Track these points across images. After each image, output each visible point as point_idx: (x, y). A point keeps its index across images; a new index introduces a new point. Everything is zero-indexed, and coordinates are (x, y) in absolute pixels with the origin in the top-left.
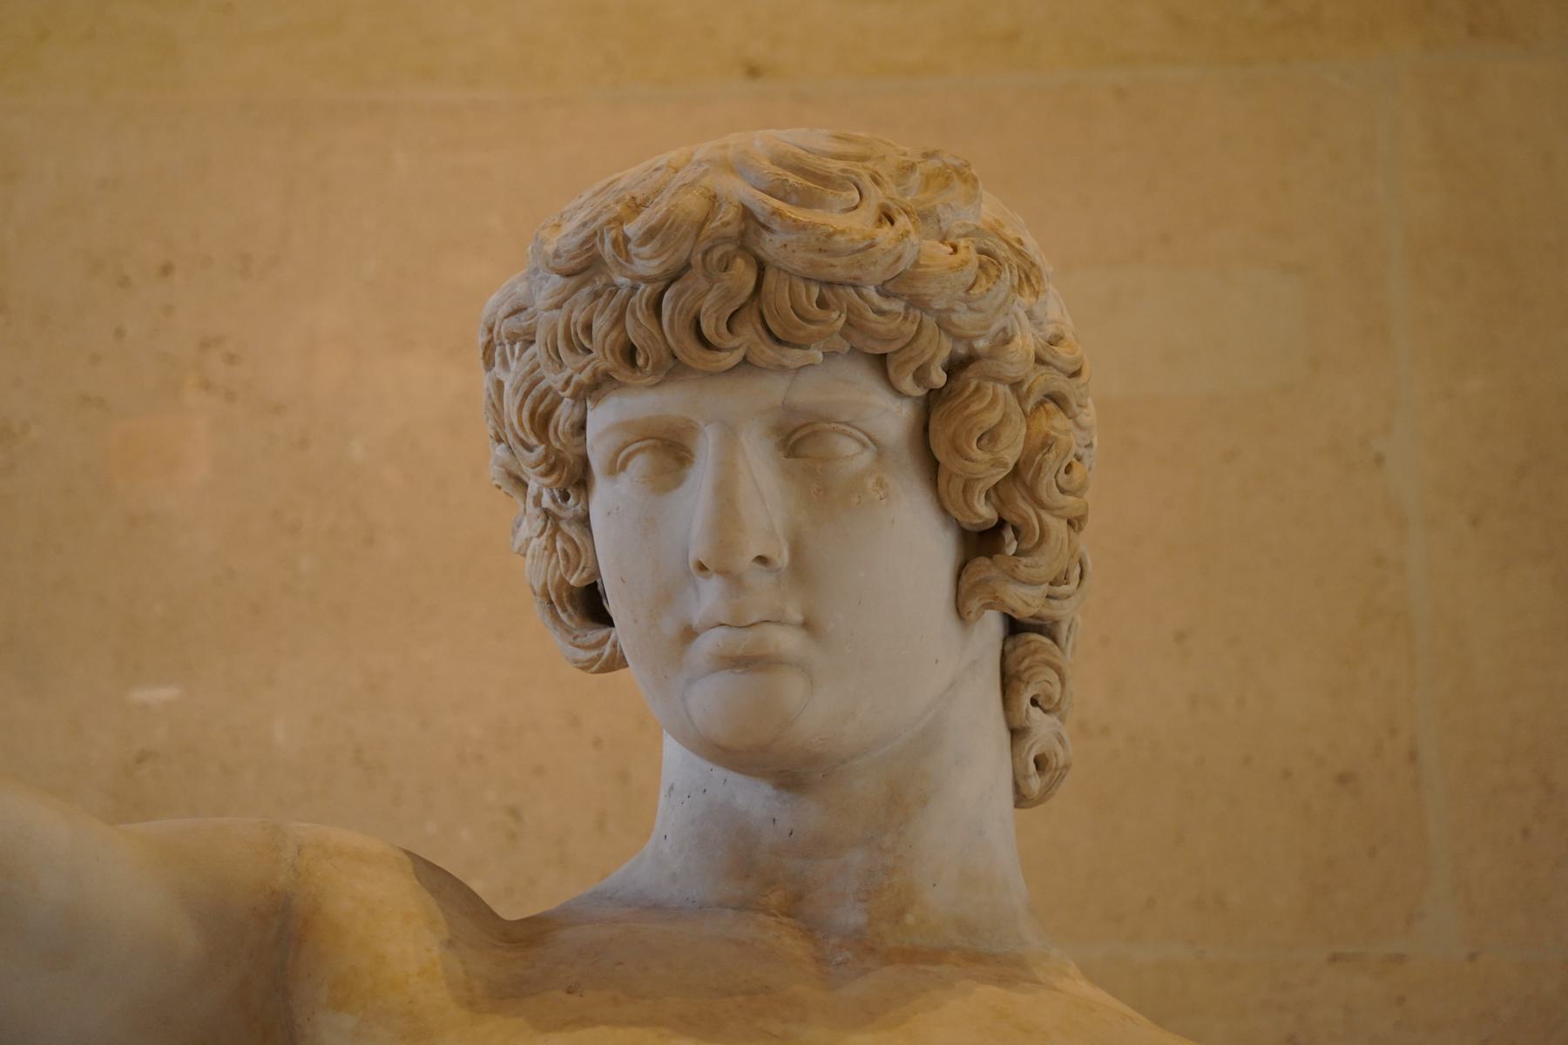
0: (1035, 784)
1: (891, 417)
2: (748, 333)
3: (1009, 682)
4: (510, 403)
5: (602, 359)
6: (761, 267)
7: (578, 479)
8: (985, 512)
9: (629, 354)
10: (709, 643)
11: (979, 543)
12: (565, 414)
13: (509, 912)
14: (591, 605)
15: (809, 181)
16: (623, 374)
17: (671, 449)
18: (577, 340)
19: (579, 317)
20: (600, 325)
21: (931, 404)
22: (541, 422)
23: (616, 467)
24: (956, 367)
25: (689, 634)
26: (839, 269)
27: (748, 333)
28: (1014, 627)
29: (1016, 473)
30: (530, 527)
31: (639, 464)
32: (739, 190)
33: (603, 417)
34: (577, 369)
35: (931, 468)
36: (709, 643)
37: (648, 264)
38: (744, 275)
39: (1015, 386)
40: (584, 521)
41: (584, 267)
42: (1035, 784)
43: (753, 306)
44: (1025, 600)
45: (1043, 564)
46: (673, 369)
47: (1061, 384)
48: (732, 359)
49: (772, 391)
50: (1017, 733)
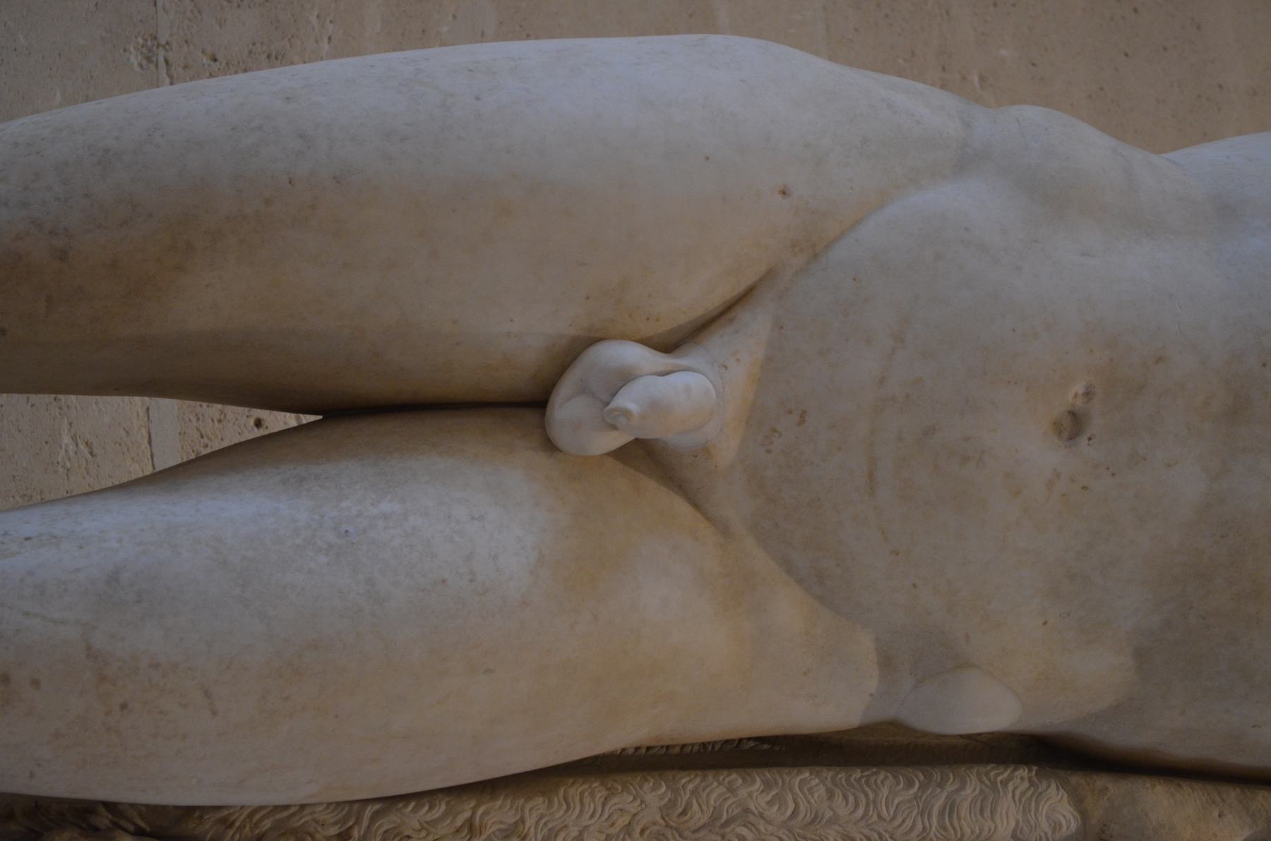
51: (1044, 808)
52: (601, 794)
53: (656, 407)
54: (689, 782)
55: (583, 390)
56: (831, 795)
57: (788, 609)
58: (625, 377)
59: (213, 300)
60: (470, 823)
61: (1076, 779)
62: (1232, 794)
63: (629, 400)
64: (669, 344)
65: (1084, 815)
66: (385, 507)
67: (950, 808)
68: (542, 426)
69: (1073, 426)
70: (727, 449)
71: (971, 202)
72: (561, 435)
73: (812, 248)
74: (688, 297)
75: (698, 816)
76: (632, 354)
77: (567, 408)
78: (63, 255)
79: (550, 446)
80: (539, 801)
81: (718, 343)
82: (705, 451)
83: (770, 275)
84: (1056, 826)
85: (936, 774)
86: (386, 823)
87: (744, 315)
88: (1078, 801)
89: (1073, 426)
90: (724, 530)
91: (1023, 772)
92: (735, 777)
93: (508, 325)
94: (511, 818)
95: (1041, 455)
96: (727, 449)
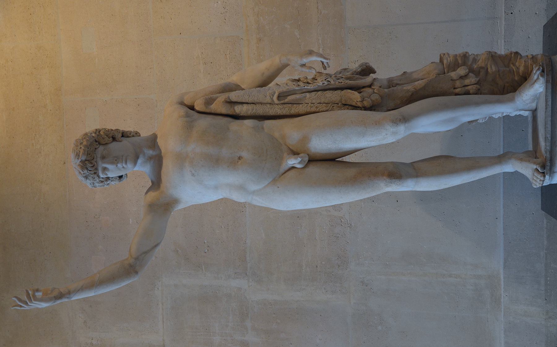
1: (101, 148)
2: (92, 162)
3: (128, 137)
4: (100, 185)
5: (95, 176)
6: (86, 160)
7: (108, 178)
8: (111, 139)
9: (95, 173)
10: (124, 165)
11: (114, 139)
12: (101, 179)
13: (151, 184)
14: (121, 177)
15: (77, 155)
17: (105, 169)
18: (94, 178)
21: (100, 144)
22: (102, 182)
23: (107, 175)
24: (96, 141)
25: (123, 167)
27: (92, 162)
28: (122, 136)
30: (113, 183)
32: (78, 162)
33: (101, 176)
34: (97, 178)
35: (106, 144)
36: (124, 165)
38: (86, 162)
41: (86, 177)
43: (90, 161)
44: (120, 135)
46: (96, 169)
49: (99, 159)
50: (133, 136)
53: (296, 159)
54: (288, 113)
55: (304, 161)
57: (277, 135)
58: (299, 163)
59: (351, 172)
61: (234, 114)
62: (213, 112)
63: (300, 159)
64: (293, 168)
67: (253, 110)
69: (240, 158)
70: (285, 155)
71: (253, 187)
72: (307, 156)
75: (287, 109)
76: (298, 166)
77: (307, 159)
78: (369, 177)
79: (308, 155)
80: (308, 111)
81: (287, 168)
87: (283, 171)
89: (240, 158)
90: (286, 145)
92: (281, 114)
93: (314, 169)
95: (245, 154)
96: (285, 155)
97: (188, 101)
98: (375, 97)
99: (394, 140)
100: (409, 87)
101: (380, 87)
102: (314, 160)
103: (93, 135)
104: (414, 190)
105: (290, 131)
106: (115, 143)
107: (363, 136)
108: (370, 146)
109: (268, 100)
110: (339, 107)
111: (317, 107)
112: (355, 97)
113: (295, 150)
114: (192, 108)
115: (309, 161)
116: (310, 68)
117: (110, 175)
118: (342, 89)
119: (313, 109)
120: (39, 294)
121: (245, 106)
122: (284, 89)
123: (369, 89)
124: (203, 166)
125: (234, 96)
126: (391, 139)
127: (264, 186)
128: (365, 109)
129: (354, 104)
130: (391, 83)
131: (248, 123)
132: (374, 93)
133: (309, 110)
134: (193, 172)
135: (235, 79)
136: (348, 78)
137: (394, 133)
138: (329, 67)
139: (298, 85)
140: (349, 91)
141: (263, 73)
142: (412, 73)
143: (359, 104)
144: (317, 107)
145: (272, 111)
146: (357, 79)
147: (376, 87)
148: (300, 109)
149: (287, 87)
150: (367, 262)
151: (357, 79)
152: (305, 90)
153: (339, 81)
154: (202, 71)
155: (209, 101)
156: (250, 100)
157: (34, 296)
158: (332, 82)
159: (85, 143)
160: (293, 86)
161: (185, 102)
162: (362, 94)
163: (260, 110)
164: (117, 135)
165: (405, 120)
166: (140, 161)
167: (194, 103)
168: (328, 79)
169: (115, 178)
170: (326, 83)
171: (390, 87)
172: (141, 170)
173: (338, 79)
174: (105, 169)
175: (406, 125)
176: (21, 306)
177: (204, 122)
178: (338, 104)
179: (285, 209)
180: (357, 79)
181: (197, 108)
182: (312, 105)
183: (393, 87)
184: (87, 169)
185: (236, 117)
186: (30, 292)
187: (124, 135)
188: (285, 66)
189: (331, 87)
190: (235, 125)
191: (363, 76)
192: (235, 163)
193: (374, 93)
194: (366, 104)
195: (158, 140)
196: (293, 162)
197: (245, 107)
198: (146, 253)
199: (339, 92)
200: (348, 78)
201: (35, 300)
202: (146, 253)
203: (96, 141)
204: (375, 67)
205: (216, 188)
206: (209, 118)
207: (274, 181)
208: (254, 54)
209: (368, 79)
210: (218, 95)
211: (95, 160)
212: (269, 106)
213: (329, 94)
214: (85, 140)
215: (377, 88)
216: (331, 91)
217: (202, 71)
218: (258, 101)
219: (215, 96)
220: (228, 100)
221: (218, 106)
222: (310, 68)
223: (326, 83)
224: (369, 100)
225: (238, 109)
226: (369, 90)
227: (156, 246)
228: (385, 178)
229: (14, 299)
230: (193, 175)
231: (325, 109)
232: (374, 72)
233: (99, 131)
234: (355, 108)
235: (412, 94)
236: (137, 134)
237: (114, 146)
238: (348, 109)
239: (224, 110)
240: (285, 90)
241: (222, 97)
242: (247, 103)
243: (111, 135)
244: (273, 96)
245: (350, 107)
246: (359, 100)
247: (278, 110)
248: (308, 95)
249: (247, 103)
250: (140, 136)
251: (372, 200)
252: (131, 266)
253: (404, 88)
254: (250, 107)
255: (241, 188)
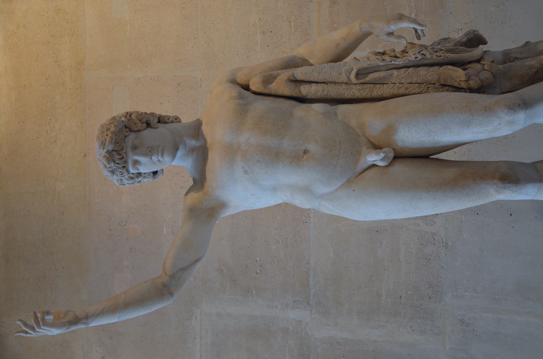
0: (178, 120)
1: (132, 136)
2: (121, 152)
3: (166, 123)
5: (124, 171)
6: (113, 150)
7: (139, 174)
8: (145, 125)
9: (124, 167)
10: (160, 158)
11: (148, 125)
14: (155, 173)
15: (103, 144)
16: (126, 168)
17: (136, 162)
18: (122, 174)
19: (119, 173)
20: (120, 170)
21: (131, 130)
22: (132, 178)
23: (138, 170)
24: (126, 127)
25: (159, 161)
26: (114, 141)
27: (121, 152)
28: (159, 122)
29: (140, 120)
30: (145, 180)
31: (137, 166)
34: (125, 173)
35: (139, 131)
36: (160, 158)
37: (112, 165)
39: (129, 120)
40: (145, 173)
41: (113, 172)
42: (178, 120)
43: (118, 152)
44: (156, 120)
45: (151, 118)
46: (126, 162)
47: (129, 115)
48: (125, 155)
50: (172, 122)
51: (306, 91)
52: (384, 94)
53: (378, 154)
54: (368, 96)
56: (344, 93)
57: (353, 123)
58: (382, 160)
59: (450, 173)
60: (407, 90)
62: (273, 93)
63: (382, 155)
64: (374, 166)
65: (299, 90)
66: (422, 139)
67: (323, 91)
68: (395, 154)
70: (364, 149)
71: (322, 189)
72: (392, 151)
73: (349, 183)
74: (372, 173)
75: (367, 90)
76: (381, 164)
77: (392, 155)
78: (474, 180)
79: (394, 150)
81: (366, 166)
82: (368, 148)
83: (356, 177)
84: (304, 88)
85: (325, 97)
86: (421, 90)
87: (361, 170)
88: (300, 92)
89: (305, 152)
90: (364, 136)
91: (309, 97)
92: (360, 97)
93: (401, 169)
94: (400, 90)
95: (312, 147)
96: (364, 149)
97: (241, 79)
98: (485, 75)
99: (510, 132)
100: (534, 62)
101: (493, 62)
102: (401, 156)
103: (123, 119)
104: (536, 199)
105: (371, 119)
106: (149, 130)
107: (468, 126)
108: (476, 139)
109: (344, 78)
110: (436, 88)
111: (407, 89)
112: (458, 75)
113: (377, 143)
114: (246, 88)
115: (395, 158)
116: (400, 37)
117: (142, 170)
118: (440, 64)
119: (402, 91)
120: (49, 318)
121: (314, 86)
122: (365, 64)
123: (477, 64)
124: (258, 161)
125: (300, 73)
126: (505, 131)
127: (335, 188)
128: (471, 90)
129: (456, 84)
130: (508, 57)
131: (318, 107)
132: (484, 69)
133: (396, 91)
134: (246, 168)
135: (301, 51)
136: (448, 51)
137: (510, 123)
138: (424, 35)
139: (383, 60)
140: (450, 67)
141: (338, 45)
142: (537, 43)
143: (463, 85)
144: (407, 89)
145: (348, 94)
146: (461, 51)
147: (486, 62)
148: (385, 90)
149: (369, 62)
150: (468, 294)
151: (461, 51)
152: (391, 66)
153: (437, 54)
154: (259, 42)
155: (268, 80)
156: (321, 78)
157: (43, 320)
158: (428, 56)
159: (112, 129)
160: (376, 61)
161: (238, 80)
162: (467, 71)
163: (333, 91)
164: (152, 120)
165: (526, 105)
166: (179, 153)
167: (249, 81)
168: (422, 52)
169: (149, 174)
170: (420, 57)
171: (505, 62)
172: (182, 164)
173: (436, 52)
174: (136, 162)
175: (528, 112)
176: (27, 333)
177: (261, 106)
178: (434, 84)
179: (361, 219)
180: (461, 51)
181: (253, 88)
182: (401, 85)
183: (510, 62)
184: (114, 161)
185: (302, 100)
186: (39, 315)
187: (161, 120)
188: (366, 35)
189: (426, 62)
190: (300, 110)
191: (469, 47)
192: (299, 158)
193: (484, 69)
194: (472, 84)
195: (203, 128)
196: (374, 158)
197: (314, 87)
198: (184, 269)
199: (436, 68)
200: (448, 51)
201: (44, 325)
202: (184, 269)
203: (126, 127)
204: (485, 35)
205: (275, 189)
206: (267, 102)
207: (349, 183)
208: (326, 21)
209: (477, 52)
210: (279, 71)
211: (124, 151)
212: (344, 86)
213: (423, 71)
214: (112, 125)
215: (489, 63)
216: (426, 68)
217: (259, 42)
218: (330, 80)
219: (275, 72)
220: (293, 79)
221: (279, 86)
222: (400, 37)
223: (420, 57)
224: (477, 79)
225: (305, 90)
226: (478, 66)
227: (197, 261)
228: (495, 181)
229: (19, 323)
230: (246, 172)
231: (417, 90)
232: (485, 43)
233: (131, 115)
234: (458, 89)
235: (537, 72)
236: (177, 120)
237: (148, 133)
238: (448, 90)
239: (286, 90)
240: (365, 65)
241: (285, 75)
242: (317, 83)
243: (144, 120)
244: (350, 73)
245: (451, 89)
246: (463, 78)
247: (356, 92)
248: (395, 72)
249: (317, 83)
250: (180, 122)
251: (476, 211)
252: (164, 285)
253: (526, 63)
254: (320, 87)
255: (306, 190)
